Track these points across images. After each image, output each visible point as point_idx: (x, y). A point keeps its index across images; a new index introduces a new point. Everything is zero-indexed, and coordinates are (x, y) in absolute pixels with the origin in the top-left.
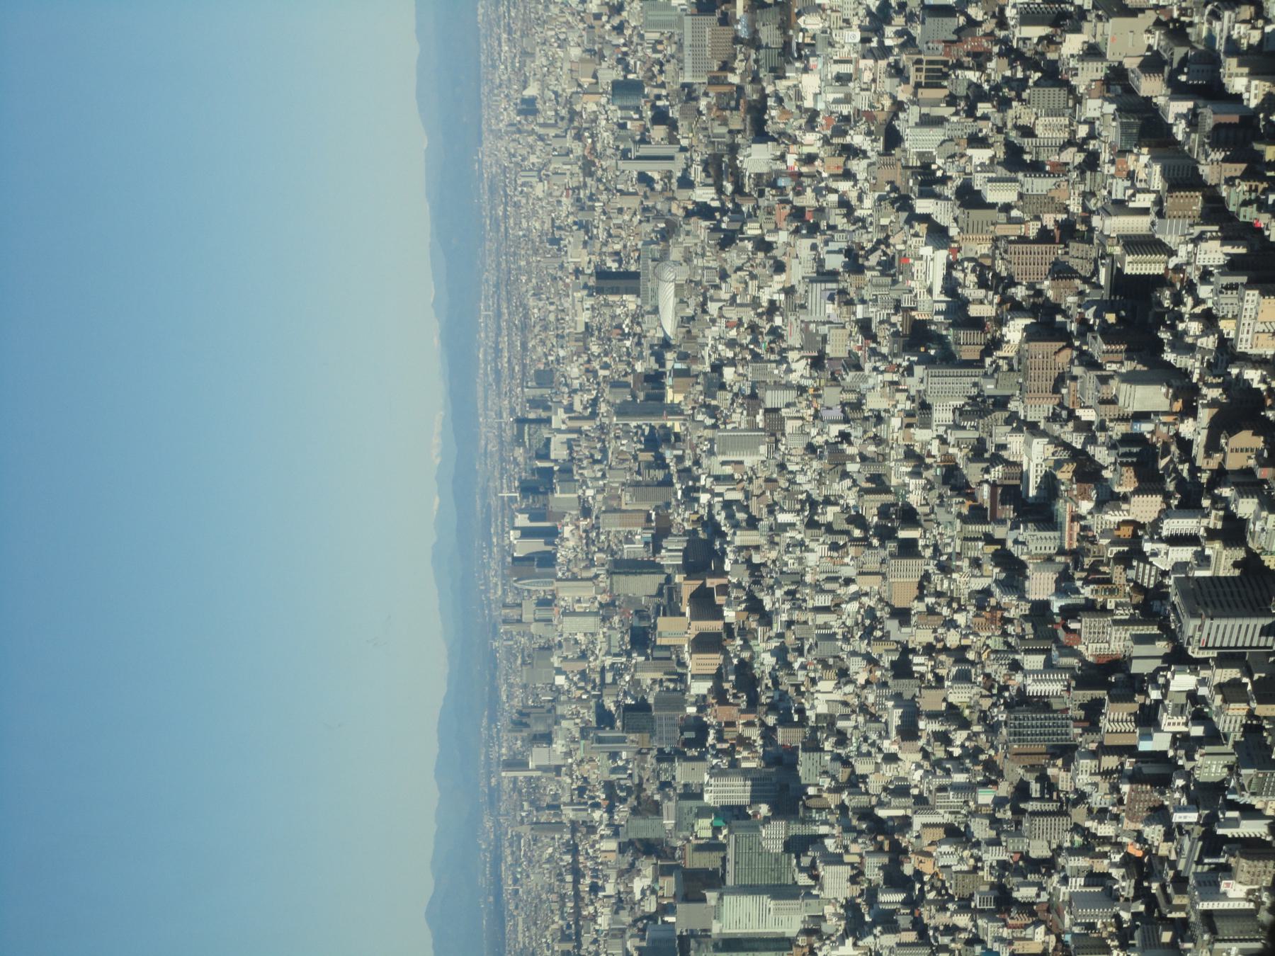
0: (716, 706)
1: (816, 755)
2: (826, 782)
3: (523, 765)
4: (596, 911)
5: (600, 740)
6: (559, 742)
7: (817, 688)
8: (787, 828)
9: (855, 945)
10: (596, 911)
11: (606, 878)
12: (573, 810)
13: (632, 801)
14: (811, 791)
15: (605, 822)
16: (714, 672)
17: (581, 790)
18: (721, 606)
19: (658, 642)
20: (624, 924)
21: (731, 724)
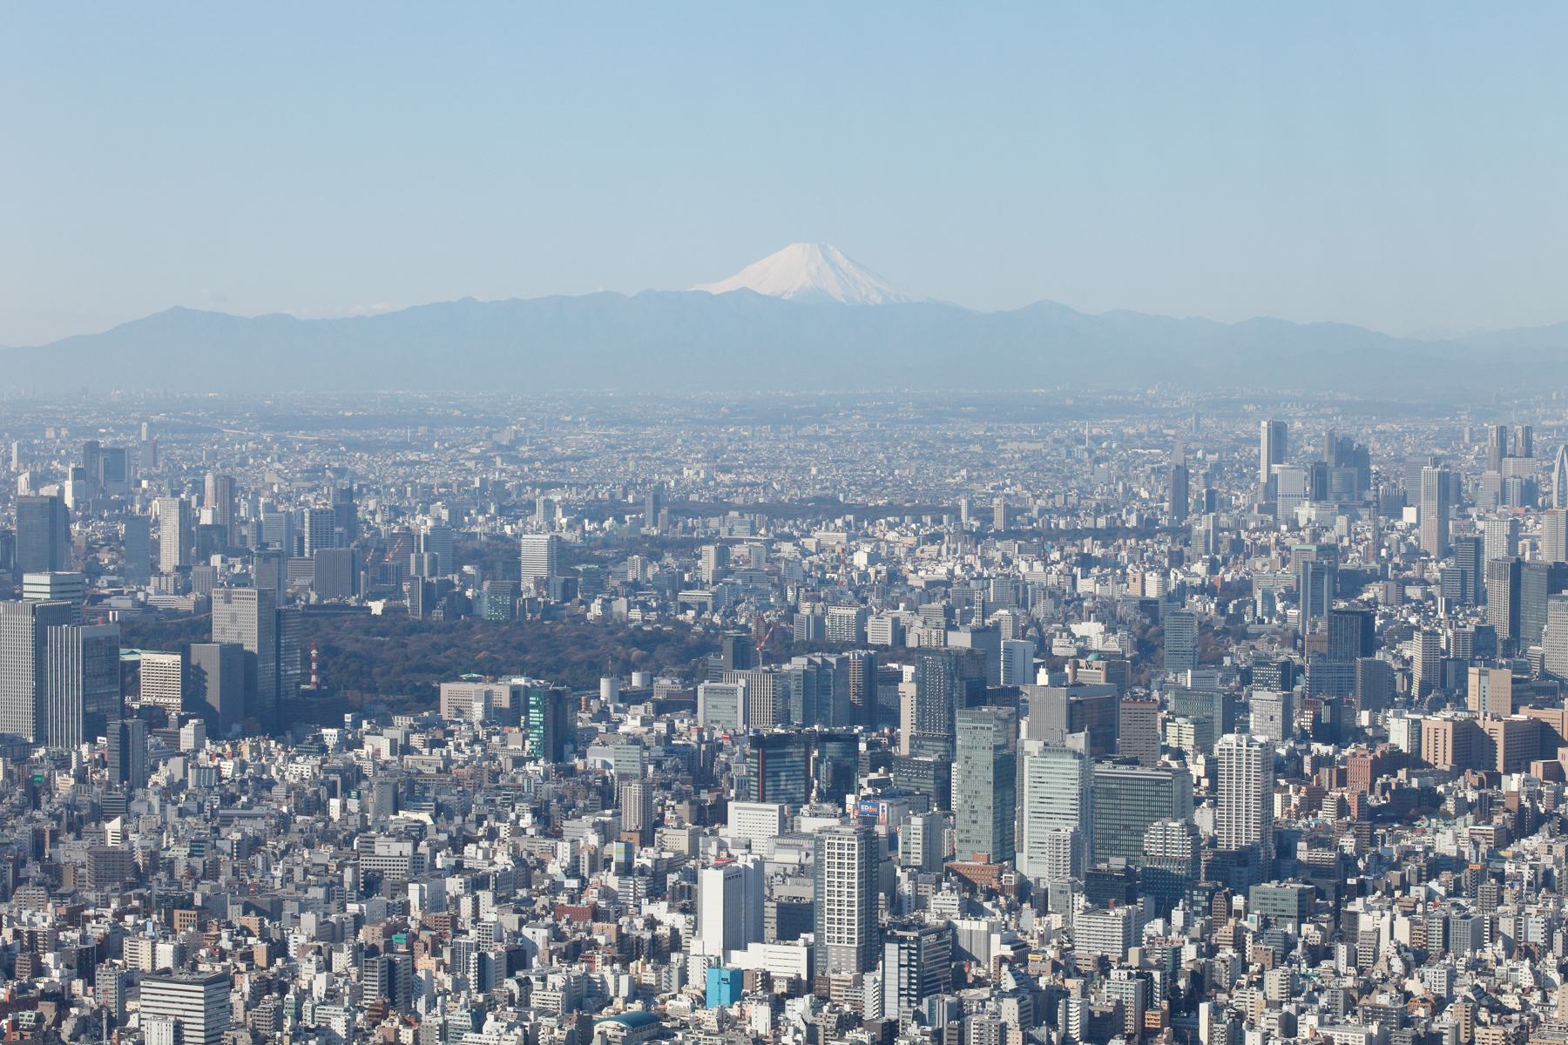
0: (1370, 758)
1: (1293, 909)
2: (1251, 923)
3: (1277, 454)
4: (1053, 563)
5: (1318, 573)
6: (1313, 512)
7: (1399, 916)
8: (1180, 862)
9: (1003, 959)
10: (1053, 563)
11: (1102, 580)
12: (1208, 532)
13: (1220, 623)
14: (1238, 901)
15: (1188, 580)
16: (1424, 757)
17: (1237, 546)
18: (1528, 771)
19: (1471, 670)
20: (1033, 605)
21: (1342, 780)
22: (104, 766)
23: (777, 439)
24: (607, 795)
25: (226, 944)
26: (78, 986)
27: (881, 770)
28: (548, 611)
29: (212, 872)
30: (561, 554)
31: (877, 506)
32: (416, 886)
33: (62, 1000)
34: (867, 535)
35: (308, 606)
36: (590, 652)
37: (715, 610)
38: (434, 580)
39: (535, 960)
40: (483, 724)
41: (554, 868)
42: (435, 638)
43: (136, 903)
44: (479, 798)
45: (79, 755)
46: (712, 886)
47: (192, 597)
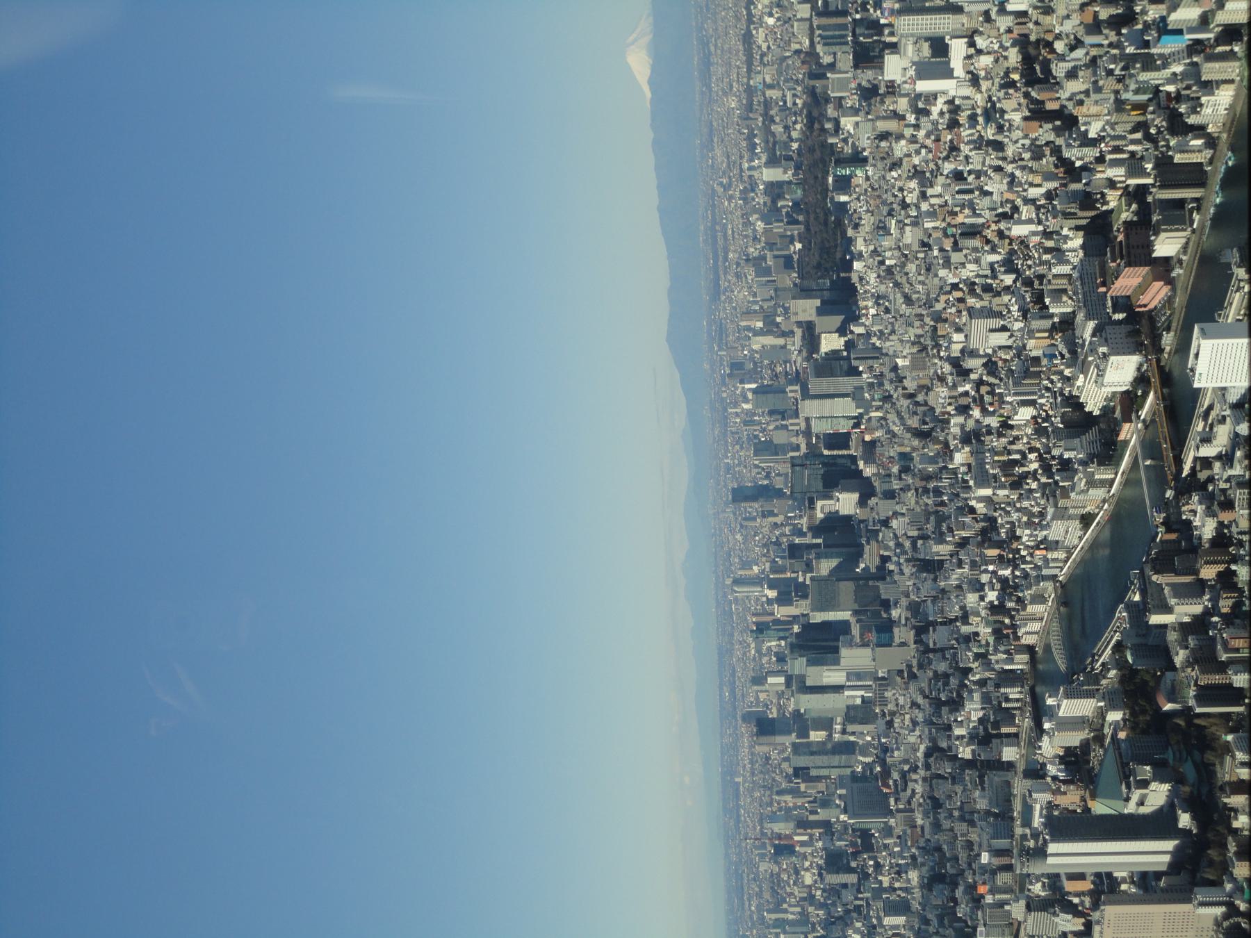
22: (872, 367)
23: (717, 63)
24: (884, 136)
25: (953, 310)
26: (973, 376)
27: (869, 7)
28: (798, 168)
29: (920, 317)
30: (773, 162)
31: (747, 14)
32: (925, 224)
33: (980, 383)
34: (760, 19)
35: (799, 277)
36: (816, 147)
37: (795, 89)
38: (785, 220)
39: (959, 168)
40: (850, 196)
41: (916, 160)
42: (812, 216)
43: (935, 351)
44: (885, 196)
45: (868, 378)
46: (924, 86)
47: (796, 329)
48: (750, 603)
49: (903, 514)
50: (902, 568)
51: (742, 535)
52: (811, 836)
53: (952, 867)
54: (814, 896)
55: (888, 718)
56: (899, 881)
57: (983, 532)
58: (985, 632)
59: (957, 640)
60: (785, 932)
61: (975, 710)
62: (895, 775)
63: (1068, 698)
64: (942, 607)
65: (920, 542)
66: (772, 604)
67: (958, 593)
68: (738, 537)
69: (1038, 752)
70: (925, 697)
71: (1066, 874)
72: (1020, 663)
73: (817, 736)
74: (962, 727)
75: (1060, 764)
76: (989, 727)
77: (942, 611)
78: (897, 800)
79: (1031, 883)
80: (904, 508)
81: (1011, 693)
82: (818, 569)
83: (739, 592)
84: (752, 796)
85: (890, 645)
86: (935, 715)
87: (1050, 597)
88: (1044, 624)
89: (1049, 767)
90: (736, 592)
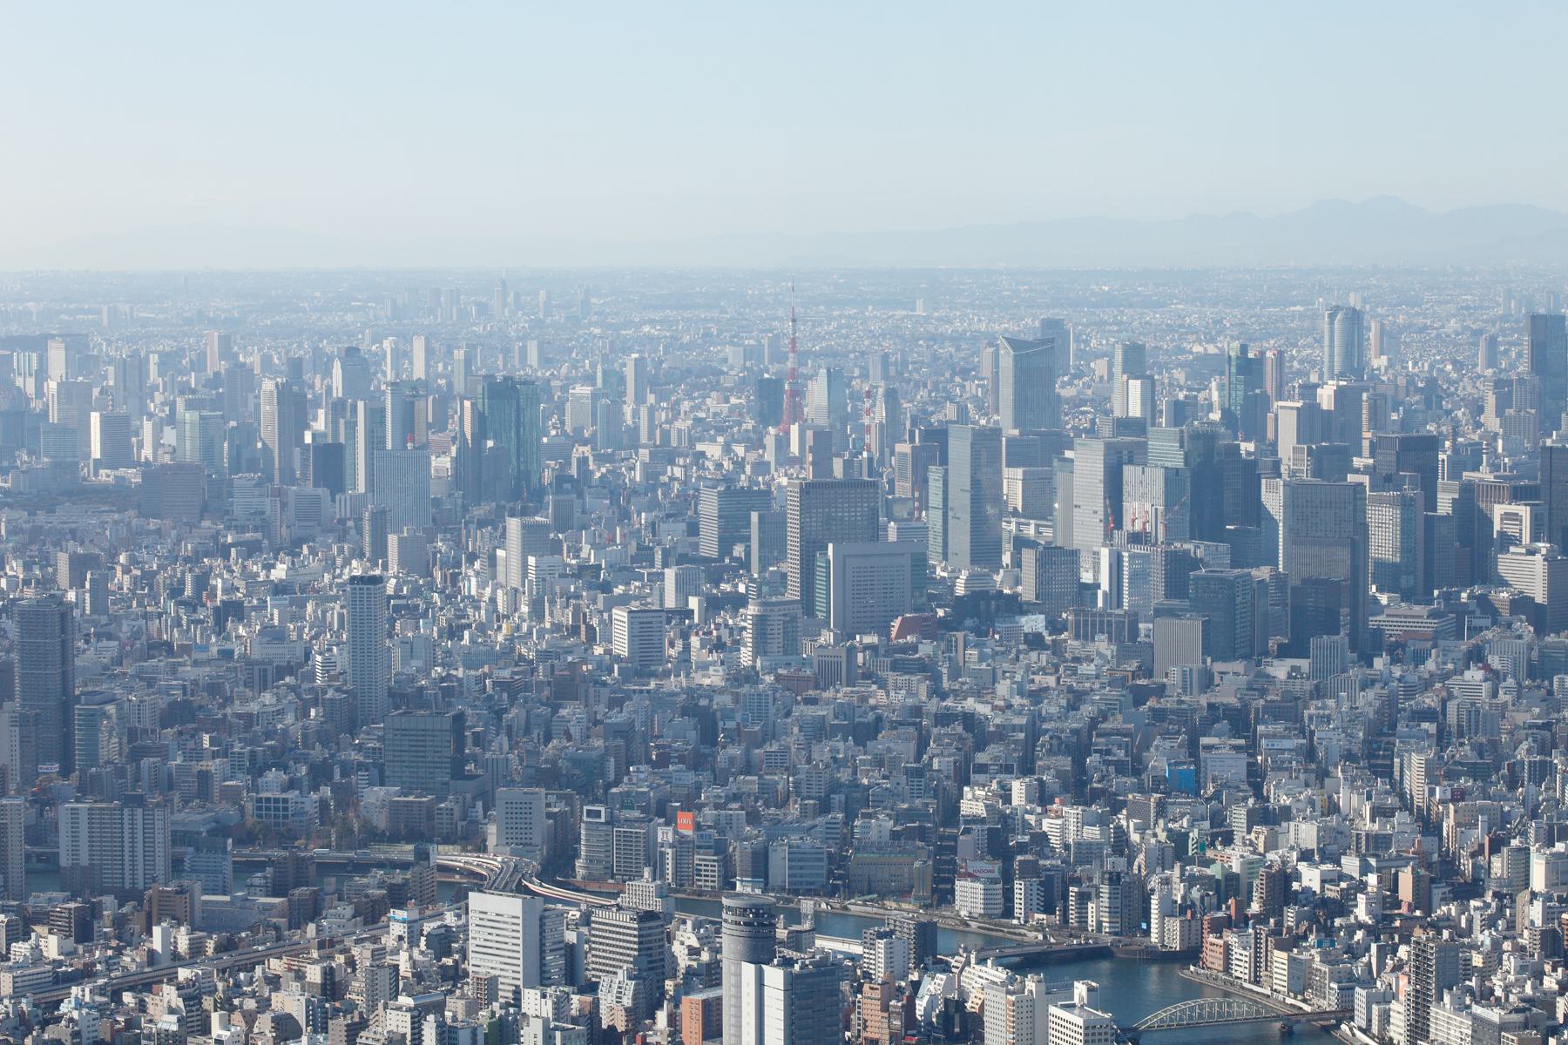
48: (1304, 346)
49: (1495, 694)
50: (1378, 686)
51: (1457, 334)
52: (799, 461)
53: (732, 760)
54: (672, 463)
55: (1048, 639)
56: (703, 647)
57: (1449, 865)
58: (1234, 859)
59: (1216, 796)
60: (595, 396)
61: (1064, 828)
62: (926, 649)
63: (1087, 1028)
64: (1289, 769)
65: (1429, 727)
66: (1302, 396)
67: (1318, 807)
68: (1453, 324)
69: (973, 957)
70: (1094, 723)
71: (719, 999)
72: (1164, 932)
73: (1013, 482)
74: (1029, 801)
75: (947, 1001)
76: (1029, 857)
77: (1279, 767)
78: (872, 648)
79: (697, 926)
80: (1508, 698)
81: (1098, 907)
82: (1380, 502)
83: (1332, 323)
84: (883, 335)
85: (1207, 650)
86: (1055, 742)
87: (1304, 1001)
88: (1246, 985)
89: (941, 978)
90: (1332, 317)
